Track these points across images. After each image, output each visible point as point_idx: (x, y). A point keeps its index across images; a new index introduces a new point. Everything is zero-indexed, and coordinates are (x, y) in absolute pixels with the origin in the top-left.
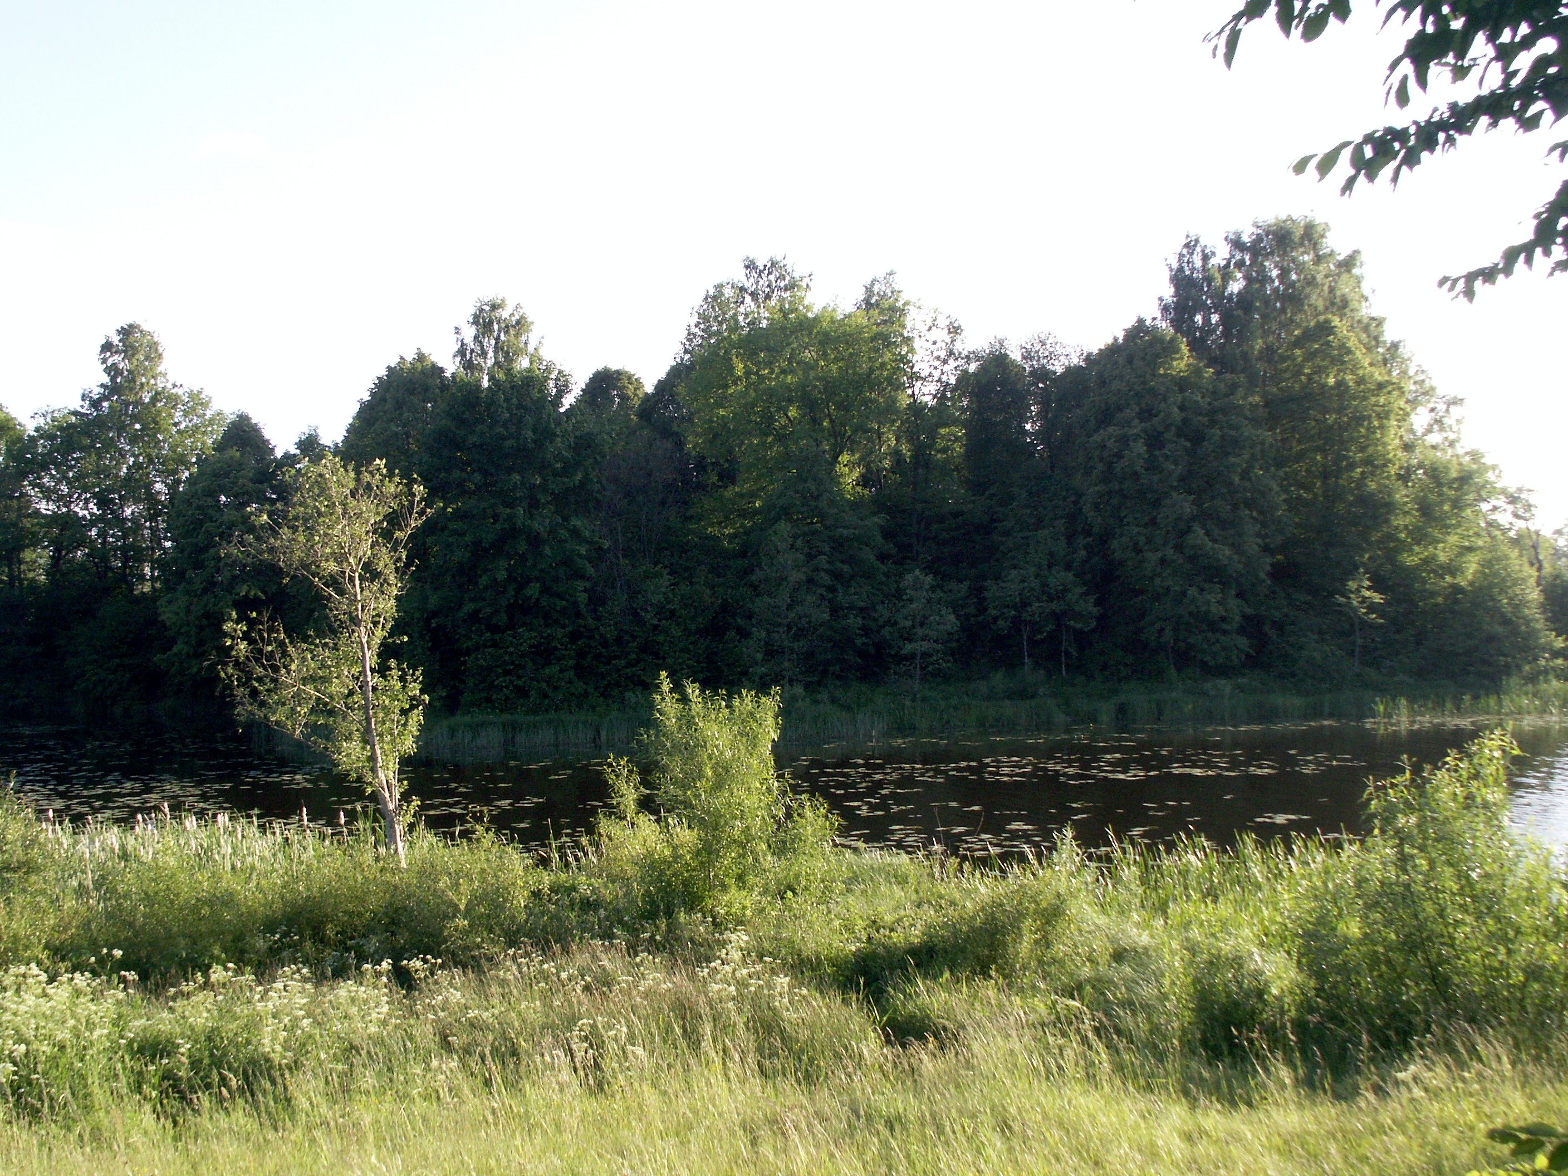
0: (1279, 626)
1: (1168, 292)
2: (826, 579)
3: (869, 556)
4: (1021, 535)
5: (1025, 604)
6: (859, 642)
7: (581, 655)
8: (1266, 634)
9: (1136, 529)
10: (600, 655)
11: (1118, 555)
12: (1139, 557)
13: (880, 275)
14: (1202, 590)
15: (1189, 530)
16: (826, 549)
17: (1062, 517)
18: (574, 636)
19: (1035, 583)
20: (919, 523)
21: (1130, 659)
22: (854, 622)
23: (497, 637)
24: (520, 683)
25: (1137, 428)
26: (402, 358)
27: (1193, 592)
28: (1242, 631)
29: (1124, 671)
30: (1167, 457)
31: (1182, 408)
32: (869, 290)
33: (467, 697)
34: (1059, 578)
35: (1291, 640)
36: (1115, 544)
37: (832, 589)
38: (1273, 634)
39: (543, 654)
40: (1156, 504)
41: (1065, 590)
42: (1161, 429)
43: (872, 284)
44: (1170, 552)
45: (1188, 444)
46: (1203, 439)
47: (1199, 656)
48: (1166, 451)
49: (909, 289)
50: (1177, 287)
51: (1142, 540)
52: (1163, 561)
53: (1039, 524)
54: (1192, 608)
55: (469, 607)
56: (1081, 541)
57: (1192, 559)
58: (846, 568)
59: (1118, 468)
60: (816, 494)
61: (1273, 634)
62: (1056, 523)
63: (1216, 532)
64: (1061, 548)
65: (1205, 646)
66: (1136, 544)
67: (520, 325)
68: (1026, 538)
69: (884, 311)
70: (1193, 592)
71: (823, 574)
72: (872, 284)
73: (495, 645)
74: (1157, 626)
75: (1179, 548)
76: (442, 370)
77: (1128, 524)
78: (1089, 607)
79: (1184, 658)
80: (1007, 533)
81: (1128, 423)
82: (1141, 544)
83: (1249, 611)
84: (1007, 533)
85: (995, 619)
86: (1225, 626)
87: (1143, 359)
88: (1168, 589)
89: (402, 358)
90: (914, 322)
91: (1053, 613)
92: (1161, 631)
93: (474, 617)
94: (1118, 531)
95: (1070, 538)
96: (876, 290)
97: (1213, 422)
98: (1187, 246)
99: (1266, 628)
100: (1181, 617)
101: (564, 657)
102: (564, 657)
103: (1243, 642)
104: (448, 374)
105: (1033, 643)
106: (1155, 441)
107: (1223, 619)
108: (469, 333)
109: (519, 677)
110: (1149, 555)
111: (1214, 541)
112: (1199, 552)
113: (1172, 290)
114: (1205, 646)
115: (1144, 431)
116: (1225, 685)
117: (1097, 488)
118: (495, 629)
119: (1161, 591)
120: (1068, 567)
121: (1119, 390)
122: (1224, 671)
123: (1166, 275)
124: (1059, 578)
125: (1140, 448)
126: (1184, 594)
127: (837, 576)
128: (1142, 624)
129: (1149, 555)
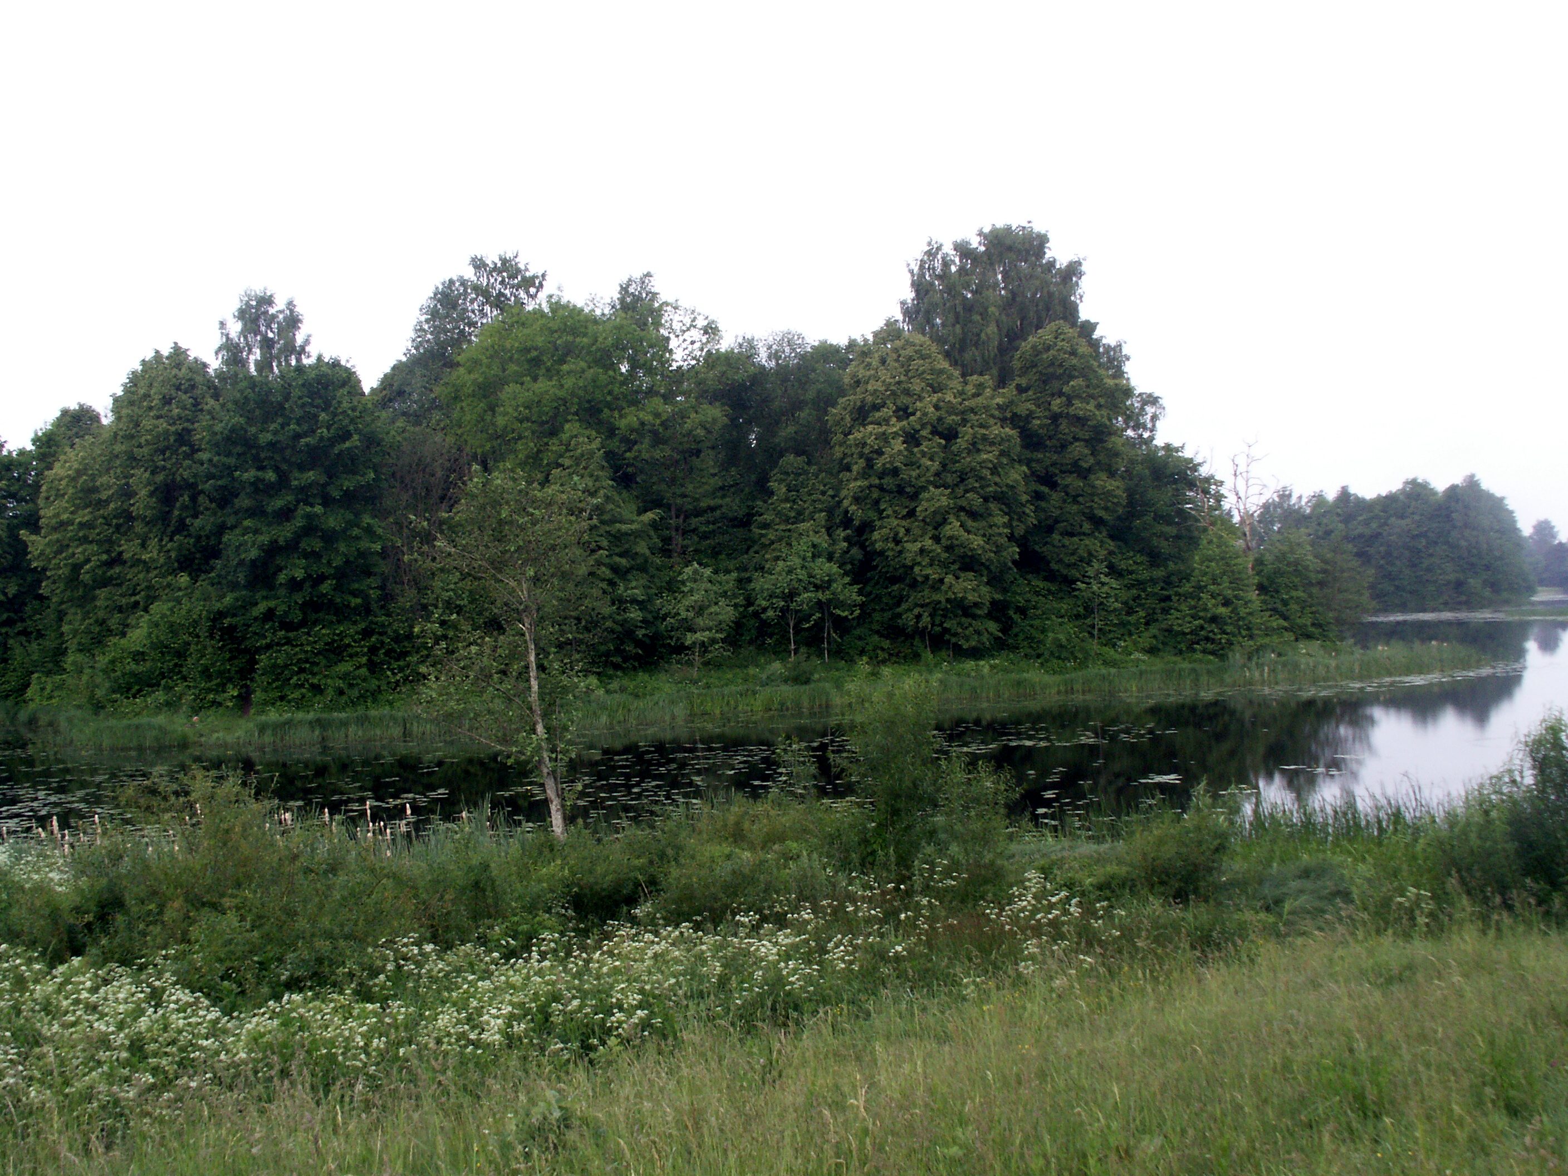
0: (1022, 611)
1: (909, 295)
2: (605, 572)
3: (642, 548)
4: (783, 527)
5: (791, 595)
6: (640, 633)
7: (373, 650)
8: (1011, 618)
9: (896, 522)
10: (393, 650)
11: (878, 546)
12: (899, 548)
13: (637, 275)
14: (957, 578)
15: (945, 521)
16: (605, 543)
17: (821, 511)
18: (367, 633)
19: (802, 574)
20: (677, 517)
21: (886, 644)
22: (635, 614)
23: (291, 635)
24: (315, 681)
25: (896, 426)
26: (157, 352)
27: (949, 579)
28: (990, 616)
29: (881, 655)
30: (924, 454)
31: (937, 407)
32: (624, 289)
33: (258, 696)
34: (823, 568)
35: (1037, 622)
36: (876, 536)
37: (611, 583)
38: (1016, 617)
39: (336, 651)
40: (915, 497)
41: (830, 582)
42: (918, 427)
43: (628, 285)
44: (928, 543)
45: (943, 442)
46: (956, 437)
47: (953, 640)
48: (922, 448)
49: (664, 289)
50: (918, 292)
51: (902, 531)
52: (922, 551)
53: (799, 517)
54: (951, 595)
55: (262, 607)
56: (841, 533)
57: (948, 549)
58: (624, 561)
59: (879, 463)
60: (593, 490)
61: (1016, 617)
62: (817, 516)
63: (970, 523)
64: (822, 540)
65: (960, 630)
66: (897, 534)
67: (293, 321)
68: (789, 530)
69: (639, 309)
70: (949, 579)
71: (604, 569)
72: (628, 285)
73: (289, 642)
74: (916, 611)
75: (937, 539)
76: (205, 365)
77: (888, 517)
78: (852, 595)
79: (939, 642)
80: (766, 526)
81: (887, 421)
82: (901, 535)
83: (998, 596)
84: (766, 526)
85: (765, 610)
86: (979, 612)
87: (897, 360)
88: (927, 577)
89: (157, 352)
90: (674, 320)
91: (819, 602)
92: (919, 617)
93: (269, 615)
94: (878, 523)
95: (829, 531)
96: (631, 290)
97: (964, 422)
98: (929, 253)
99: (1011, 613)
100: (940, 602)
101: (357, 654)
102: (357, 654)
103: (993, 626)
104: (211, 371)
105: (798, 630)
106: (912, 439)
107: (976, 605)
108: (235, 328)
109: (314, 674)
110: (908, 546)
111: (969, 532)
112: (956, 542)
113: (913, 295)
114: (960, 630)
115: (902, 429)
116: (984, 666)
117: (859, 483)
118: (288, 626)
119: (919, 579)
120: (830, 558)
121: (876, 391)
122: (976, 653)
123: (908, 280)
124: (823, 568)
125: (898, 445)
126: (941, 581)
127: (615, 569)
128: (899, 610)
129: (908, 546)
